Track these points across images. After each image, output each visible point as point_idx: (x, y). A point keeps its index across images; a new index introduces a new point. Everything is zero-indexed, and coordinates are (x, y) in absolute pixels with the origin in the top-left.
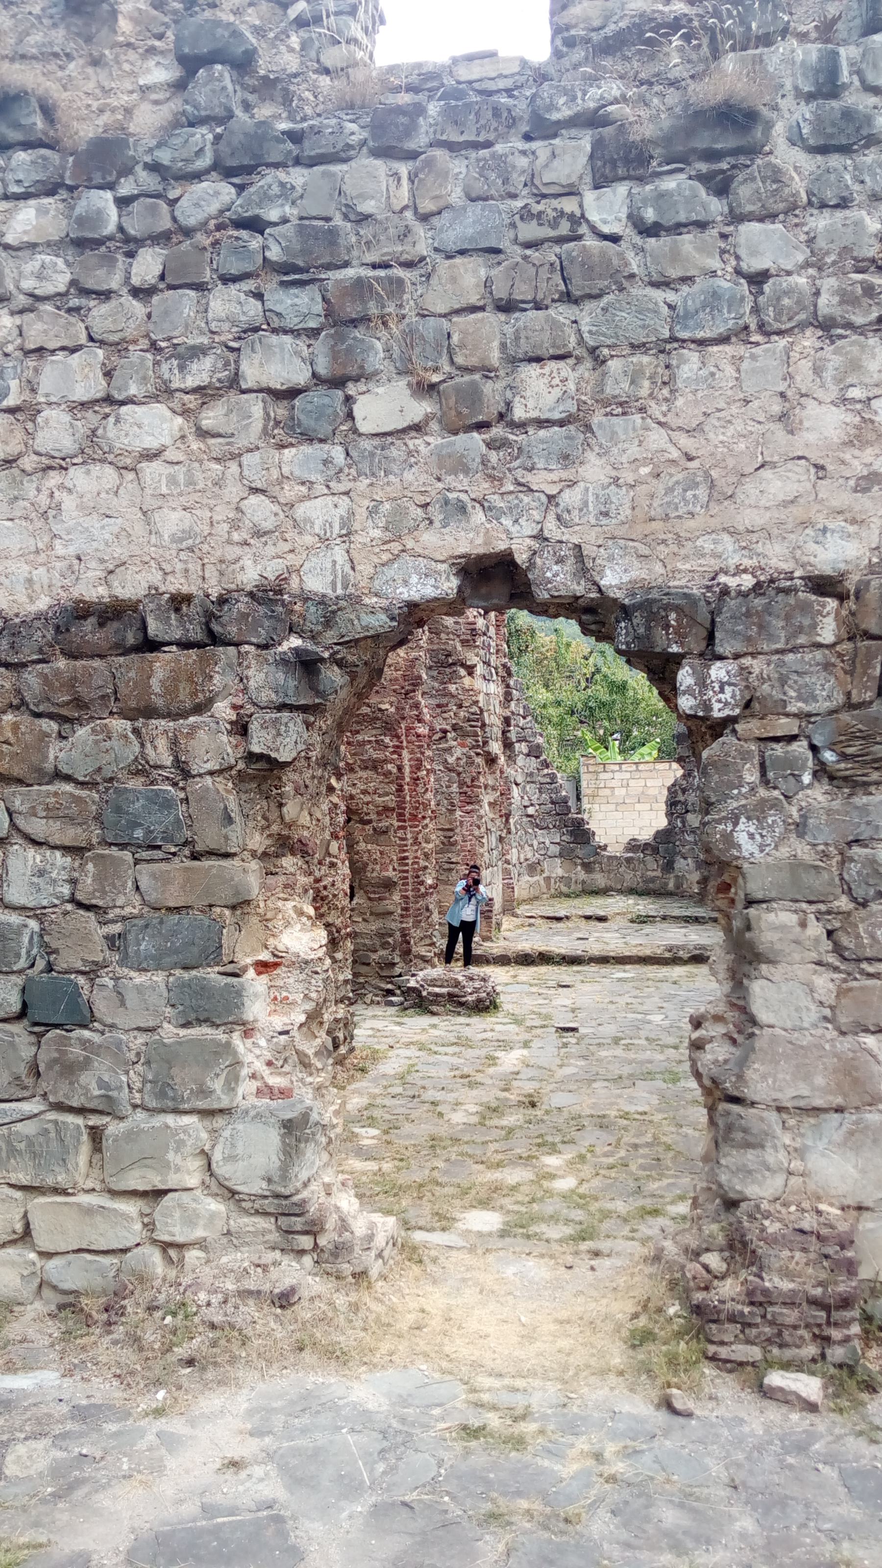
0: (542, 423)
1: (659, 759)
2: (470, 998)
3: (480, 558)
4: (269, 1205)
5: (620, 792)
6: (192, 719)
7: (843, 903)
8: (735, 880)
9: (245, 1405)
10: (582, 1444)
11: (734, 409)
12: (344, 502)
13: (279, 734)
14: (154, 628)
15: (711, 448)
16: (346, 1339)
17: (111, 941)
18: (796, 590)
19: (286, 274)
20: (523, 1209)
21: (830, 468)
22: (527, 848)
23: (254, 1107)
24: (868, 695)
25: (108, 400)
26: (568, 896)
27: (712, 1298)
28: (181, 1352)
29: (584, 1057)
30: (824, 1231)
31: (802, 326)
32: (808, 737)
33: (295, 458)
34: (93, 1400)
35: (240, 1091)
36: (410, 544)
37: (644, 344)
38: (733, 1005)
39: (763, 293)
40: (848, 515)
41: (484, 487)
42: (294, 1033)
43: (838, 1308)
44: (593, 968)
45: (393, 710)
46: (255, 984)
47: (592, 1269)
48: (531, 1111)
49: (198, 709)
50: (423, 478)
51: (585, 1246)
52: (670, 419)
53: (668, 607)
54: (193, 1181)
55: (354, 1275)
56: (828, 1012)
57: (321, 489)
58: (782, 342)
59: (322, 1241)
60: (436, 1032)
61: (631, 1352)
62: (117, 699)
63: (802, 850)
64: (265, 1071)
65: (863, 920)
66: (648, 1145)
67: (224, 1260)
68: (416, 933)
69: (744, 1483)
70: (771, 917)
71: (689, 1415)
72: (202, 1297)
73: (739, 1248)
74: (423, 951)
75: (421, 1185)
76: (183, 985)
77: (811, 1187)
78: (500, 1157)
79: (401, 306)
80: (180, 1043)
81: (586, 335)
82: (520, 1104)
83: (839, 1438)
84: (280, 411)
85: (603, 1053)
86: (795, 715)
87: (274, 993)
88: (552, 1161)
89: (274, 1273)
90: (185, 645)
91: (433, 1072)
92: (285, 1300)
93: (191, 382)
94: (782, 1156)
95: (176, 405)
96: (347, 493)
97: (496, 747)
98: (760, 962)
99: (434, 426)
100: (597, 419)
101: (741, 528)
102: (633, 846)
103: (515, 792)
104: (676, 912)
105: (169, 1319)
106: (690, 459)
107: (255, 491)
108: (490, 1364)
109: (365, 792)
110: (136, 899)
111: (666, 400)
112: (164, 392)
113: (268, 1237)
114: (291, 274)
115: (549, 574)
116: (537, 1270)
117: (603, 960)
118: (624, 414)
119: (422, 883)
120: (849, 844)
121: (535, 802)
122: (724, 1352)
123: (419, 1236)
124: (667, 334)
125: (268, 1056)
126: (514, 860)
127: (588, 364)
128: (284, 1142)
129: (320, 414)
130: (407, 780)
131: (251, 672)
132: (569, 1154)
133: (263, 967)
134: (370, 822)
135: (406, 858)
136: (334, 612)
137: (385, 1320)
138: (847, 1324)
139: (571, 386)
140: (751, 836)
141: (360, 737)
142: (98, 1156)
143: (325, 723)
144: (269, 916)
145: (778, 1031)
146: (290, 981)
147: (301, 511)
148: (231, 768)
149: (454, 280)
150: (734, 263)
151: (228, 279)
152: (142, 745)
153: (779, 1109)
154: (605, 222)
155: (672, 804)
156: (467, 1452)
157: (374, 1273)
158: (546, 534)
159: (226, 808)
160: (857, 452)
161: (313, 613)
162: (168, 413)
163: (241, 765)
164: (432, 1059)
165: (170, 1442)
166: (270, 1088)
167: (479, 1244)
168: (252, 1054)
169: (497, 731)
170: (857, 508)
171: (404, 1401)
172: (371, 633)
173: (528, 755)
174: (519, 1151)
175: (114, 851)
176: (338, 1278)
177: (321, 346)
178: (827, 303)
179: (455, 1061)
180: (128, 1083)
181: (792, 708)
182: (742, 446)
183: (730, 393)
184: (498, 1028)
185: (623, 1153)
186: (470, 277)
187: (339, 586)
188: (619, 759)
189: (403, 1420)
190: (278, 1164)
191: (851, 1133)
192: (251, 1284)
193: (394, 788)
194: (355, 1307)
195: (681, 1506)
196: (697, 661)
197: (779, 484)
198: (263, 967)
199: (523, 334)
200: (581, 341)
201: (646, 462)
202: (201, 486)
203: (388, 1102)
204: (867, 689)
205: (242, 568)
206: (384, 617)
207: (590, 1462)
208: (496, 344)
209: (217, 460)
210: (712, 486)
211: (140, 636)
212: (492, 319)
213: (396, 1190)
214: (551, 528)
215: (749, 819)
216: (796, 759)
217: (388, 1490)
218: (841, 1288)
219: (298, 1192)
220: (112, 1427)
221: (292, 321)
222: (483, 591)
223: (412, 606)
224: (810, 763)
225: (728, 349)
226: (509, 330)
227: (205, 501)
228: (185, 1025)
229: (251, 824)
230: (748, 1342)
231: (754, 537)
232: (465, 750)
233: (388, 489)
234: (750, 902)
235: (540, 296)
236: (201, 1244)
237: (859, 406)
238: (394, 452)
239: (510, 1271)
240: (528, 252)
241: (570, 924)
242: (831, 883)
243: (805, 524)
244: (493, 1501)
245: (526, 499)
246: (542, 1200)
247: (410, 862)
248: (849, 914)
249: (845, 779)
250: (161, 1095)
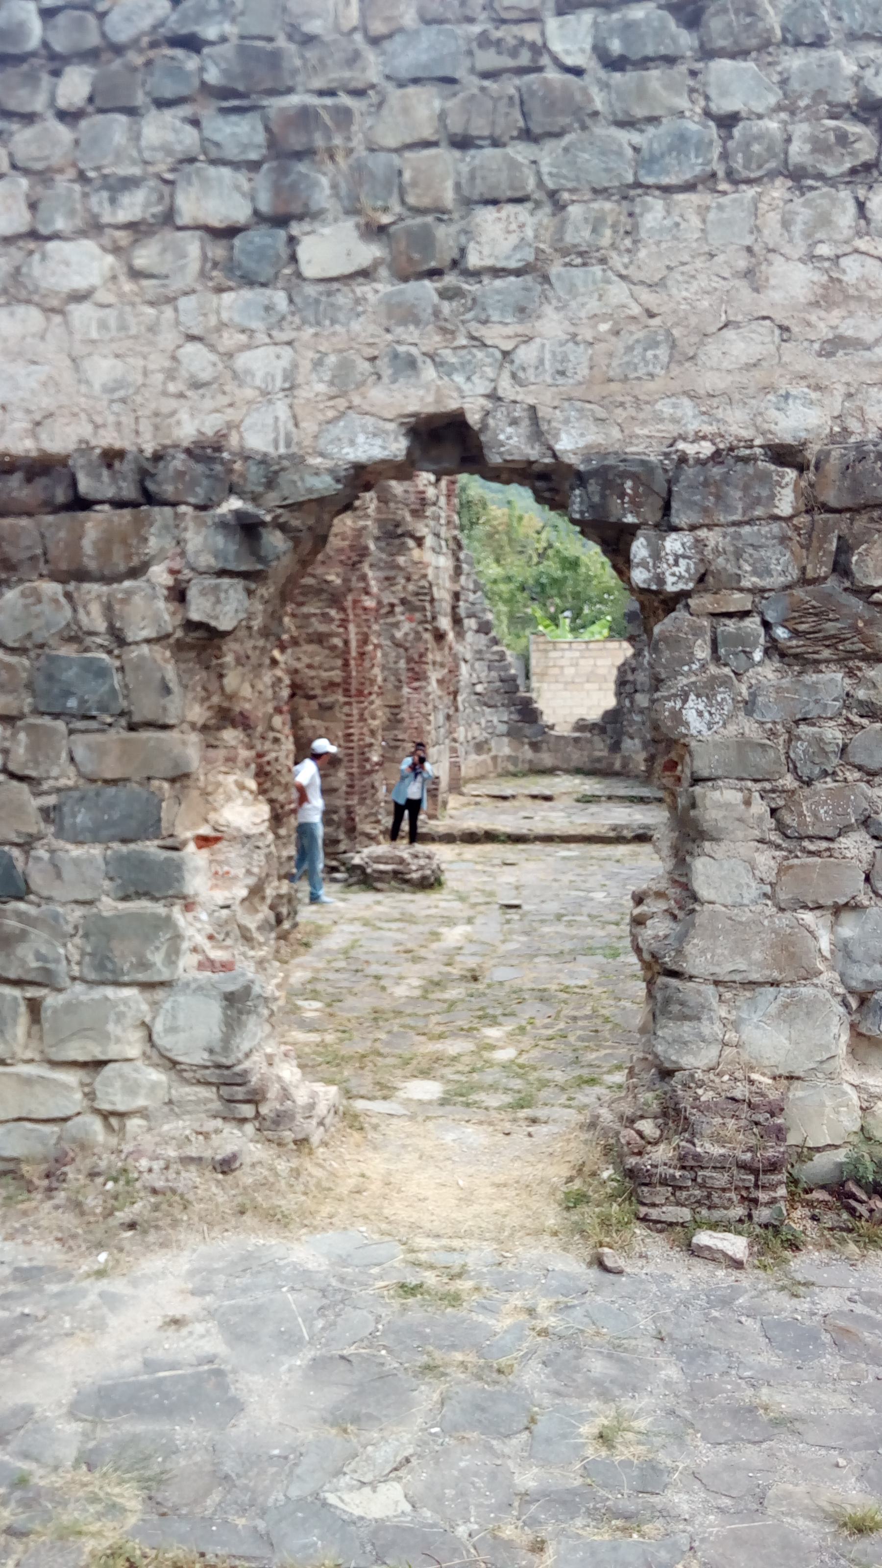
0: (497, 272)
1: (610, 638)
2: (415, 876)
3: (431, 418)
4: (211, 1075)
6: (127, 584)
7: (788, 781)
8: (682, 757)
9: (187, 1267)
10: (516, 1300)
11: (699, 263)
12: (287, 353)
13: (218, 601)
14: (85, 485)
15: (672, 305)
16: (287, 1203)
17: (46, 813)
18: (756, 459)
19: (225, 98)
20: (464, 1079)
21: (795, 329)
23: (195, 980)
24: (823, 571)
25: (33, 235)
26: (515, 775)
27: (645, 1162)
28: (123, 1216)
29: (526, 933)
30: (756, 1100)
31: (772, 175)
32: (761, 614)
33: (234, 303)
34: (35, 1263)
35: (181, 964)
36: (356, 400)
37: (606, 190)
38: (675, 882)
39: (731, 137)
40: (812, 381)
41: (434, 341)
42: (237, 907)
43: (765, 1172)
44: (538, 847)
45: (338, 581)
46: (195, 858)
47: (530, 1135)
48: (473, 985)
49: (135, 573)
50: (372, 328)
51: (523, 1113)
52: (631, 272)
53: (625, 475)
54: (134, 1051)
55: (295, 1142)
56: (768, 889)
57: (262, 338)
58: (750, 192)
59: (264, 1110)
60: (379, 909)
61: (566, 1214)
62: (47, 562)
63: (750, 728)
64: (207, 945)
65: (806, 799)
66: (586, 1017)
67: (166, 1127)
68: (361, 811)
69: (670, 1335)
70: (716, 795)
71: (620, 1272)
72: (144, 1163)
73: (672, 1116)
74: (368, 828)
75: (364, 1056)
76: (121, 859)
77: (745, 1057)
78: (442, 1028)
79: (349, 139)
80: (119, 917)
81: (546, 179)
82: (463, 978)
83: (762, 1292)
84: (218, 251)
85: (546, 929)
86: (749, 590)
87: (215, 867)
88: (493, 1033)
89: (215, 1140)
90: (118, 504)
91: (377, 947)
92: (226, 1166)
93: (122, 216)
94: (717, 1028)
95: (106, 241)
96: (289, 343)
97: (444, 623)
98: (703, 839)
99: (383, 272)
100: (555, 269)
101: (702, 392)
102: (581, 726)
103: (464, 669)
104: (622, 792)
105: (110, 1185)
106: (651, 315)
107: (192, 338)
108: (428, 1226)
109: (310, 666)
110: (71, 771)
111: (629, 251)
112: (94, 228)
113: (211, 1106)
114: (231, 98)
115: (502, 437)
116: (476, 1136)
117: (548, 839)
118: (584, 264)
119: (367, 760)
120: (797, 722)
122: (654, 1213)
123: (360, 1105)
124: (630, 179)
125: (209, 930)
126: (461, 739)
127: (548, 209)
128: (225, 1015)
129: (261, 254)
130: (354, 654)
131: (188, 535)
132: (510, 1026)
133: (204, 841)
134: (314, 697)
136: (276, 473)
137: (325, 1184)
138: (774, 1187)
139: (529, 233)
140: (700, 714)
141: (305, 610)
142: (36, 1028)
143: (266, 591)
144: (210, 789)
145: (718, 907)
146: (231, 855)
147: (242, 361)
148: (168, 636)
149: (406, 111)
150: (702, 103)
151: (162, 104)
152: (75, 610)
153: (716, 983)
154: (568, 52)
155: (621, 683)
156: (404, 1309)
157: (315, 1140)
158: (500, 393)
159: (163, 678)
160: (823, 314)
161: (255, 473)
162: (97, 251)
163: (179, 634)
164: (377, 934)
165: (111, 1300)
166: (212, 962)
167: (419, 1112)
168: (193, 928)
169: (445, 606)
170: (821, 373)
171: (343, 1261)
172: (315, 496)
174: (460, 1023)
175: (47, 721)
176: (279, 1144)
177: (263, 181)
178: (799, 152)
179: (399, 936)
180: (68, 954)
181: (746, 583)
182: (706, 303)
183: (695, 245)
184: (443, 904)
185: (562, 1025)
186: (424, 108)
187: (282, 444)
188: (570, 637)
189: (342, 1280)
190: (219, 1035)
191: (786, 1006)
192: (192, 1151)
193: (339, 662)
194: (296, 1173)
195: (610, 1356)
196: (652, 533)
197: (742, 345)
198: (204, 841)
199: (479, 174)
200: (540, 183)
201: (605, 317)
202: (133, 331)
203: (331, 976)
204: (822, 563)
205: (179, 423)
206: (328, 479)
207: (524, 1317)
208: (449, 184)
209: (152, 304)
210: (673, 345)
211: (70, 493)
212: (445, 156)
213: (337, 1060)
214: (506, 388)
215: (698, 696)
216: (748, 635)
217: (326, 1345)
218: (770, 1153)
219: (239, 1062)
220: (54, 1288)
221: (232, 152)
222: (434, 453)
223: (359, 469)
224: (762, 640)
225: (694, 198)
226: (464, 169)
227: (138, 348)
228: (126, 898)
229: (190, 695)
230: (679, 1204)
231: (715, 402)
233: (334, 340)
234: (696, 780)
235: (498, 132)
236: (142, 1112)
237: (827, 264)
238: (340, 300)
239: (449, 1137)
240: (486, 83)
241: (516, 803)
242: (777, 761)
243: (767, 389)
244: (429, 1354)
245: (480, 354)
246: (481, 1070)
248: (793, 792)
249: (796, 656)
250: (100, 967)
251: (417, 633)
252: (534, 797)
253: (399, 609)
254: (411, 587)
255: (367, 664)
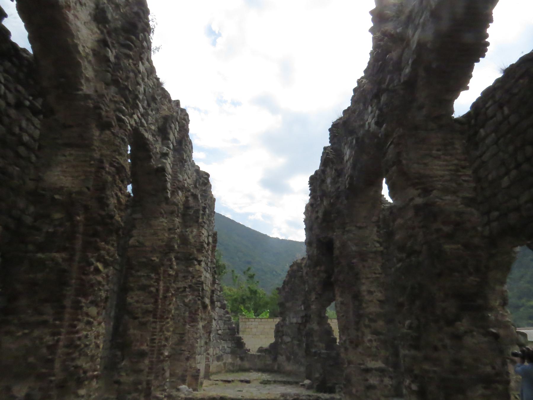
1: (270, 317)
5: (254, 330)
22: (217, 349)
26: (233, 372)
68: (155, 383)
97: (207, 301)
102: (261, 350)
103: (214, 323)
104: (280, 379)
109: (137, 302)
119: (162, 354)
121: (222, 328)
126: (211, 354)
130: (161, 297)
135: (154, 339)
141: (139, 274)
169: (208, 294)
173: (220, 308)
188: (254, 317)
193: (153, 300)
232: (194, 297)
241: (233, 384)
247: (157, 341)
251: (195, 300)
252: (242, 381)
253: (187, 290)
254: (194, 281)
255: (167, 303)
